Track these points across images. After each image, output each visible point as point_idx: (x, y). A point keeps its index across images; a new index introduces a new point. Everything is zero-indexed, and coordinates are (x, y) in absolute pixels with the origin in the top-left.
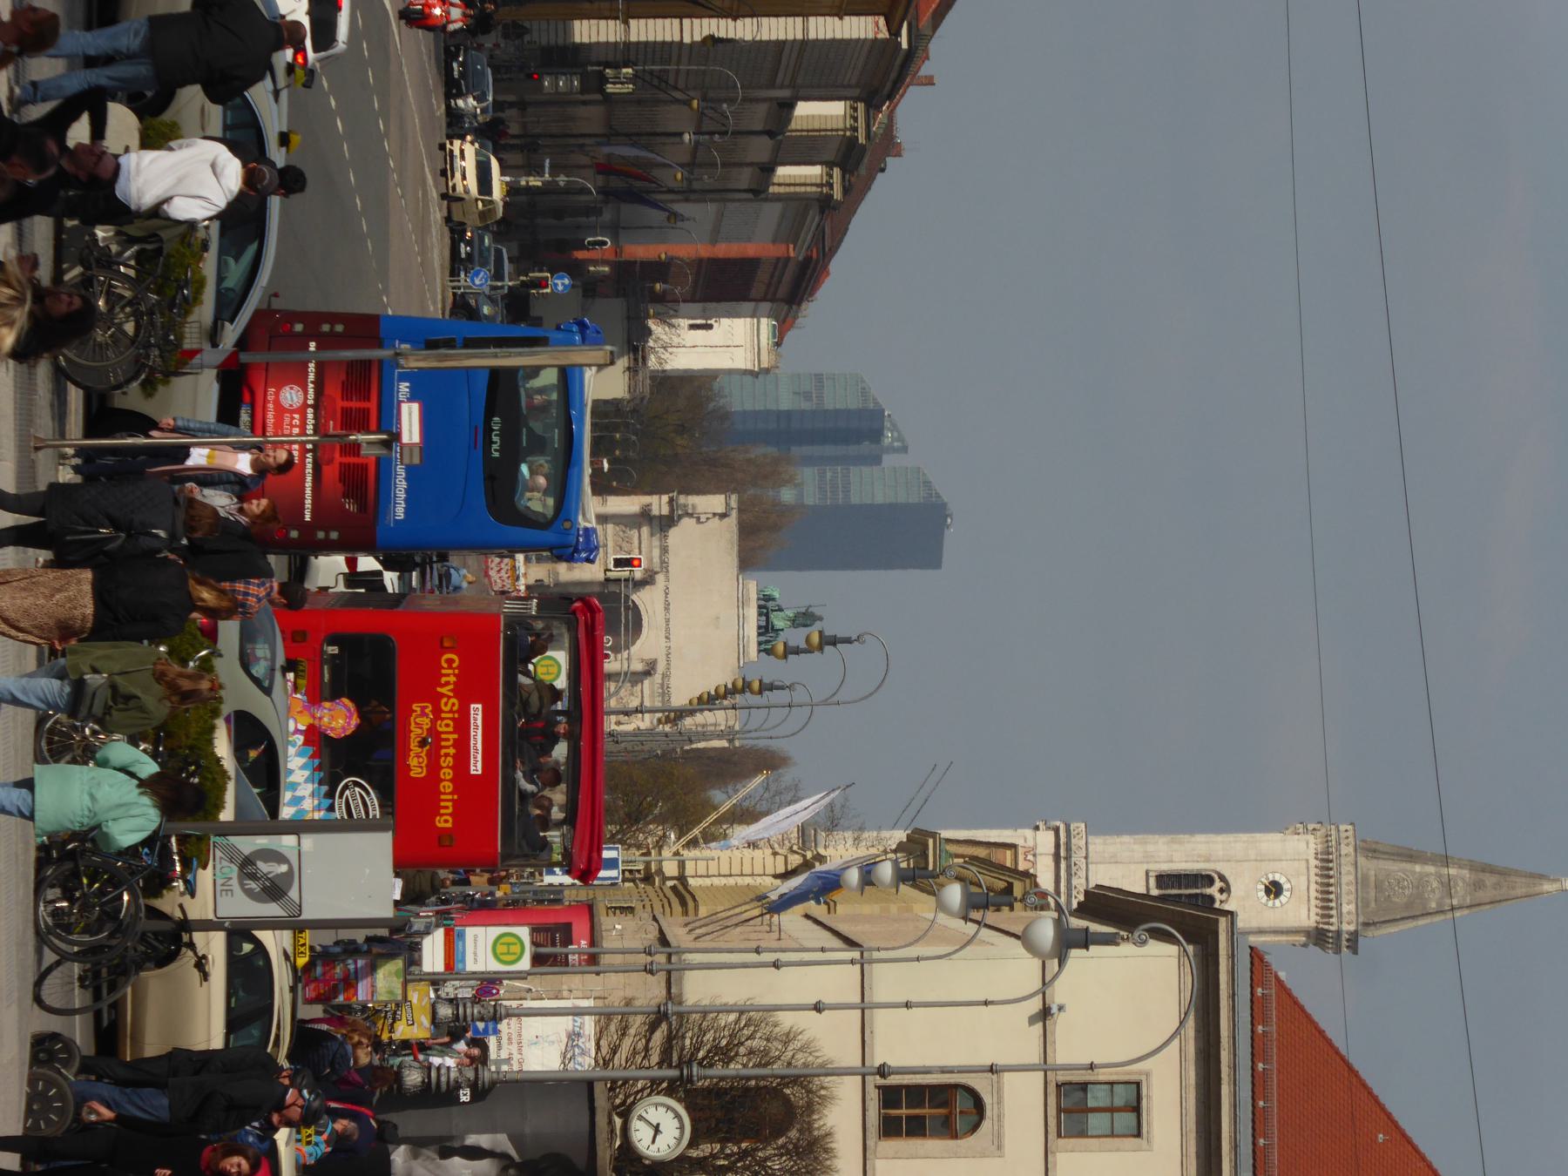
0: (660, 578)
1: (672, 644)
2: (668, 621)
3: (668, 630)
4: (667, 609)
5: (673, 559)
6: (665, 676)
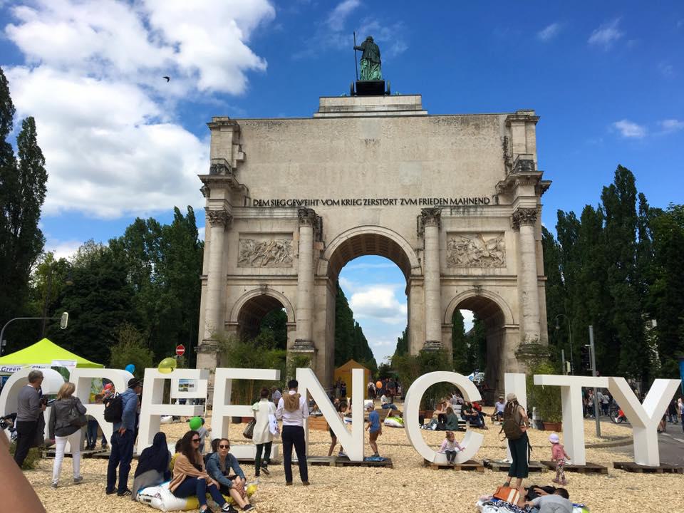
1: (399, 198)
2: (369, 202)
4: (354, 203)
5: (290, 196)
6: (442, 203)
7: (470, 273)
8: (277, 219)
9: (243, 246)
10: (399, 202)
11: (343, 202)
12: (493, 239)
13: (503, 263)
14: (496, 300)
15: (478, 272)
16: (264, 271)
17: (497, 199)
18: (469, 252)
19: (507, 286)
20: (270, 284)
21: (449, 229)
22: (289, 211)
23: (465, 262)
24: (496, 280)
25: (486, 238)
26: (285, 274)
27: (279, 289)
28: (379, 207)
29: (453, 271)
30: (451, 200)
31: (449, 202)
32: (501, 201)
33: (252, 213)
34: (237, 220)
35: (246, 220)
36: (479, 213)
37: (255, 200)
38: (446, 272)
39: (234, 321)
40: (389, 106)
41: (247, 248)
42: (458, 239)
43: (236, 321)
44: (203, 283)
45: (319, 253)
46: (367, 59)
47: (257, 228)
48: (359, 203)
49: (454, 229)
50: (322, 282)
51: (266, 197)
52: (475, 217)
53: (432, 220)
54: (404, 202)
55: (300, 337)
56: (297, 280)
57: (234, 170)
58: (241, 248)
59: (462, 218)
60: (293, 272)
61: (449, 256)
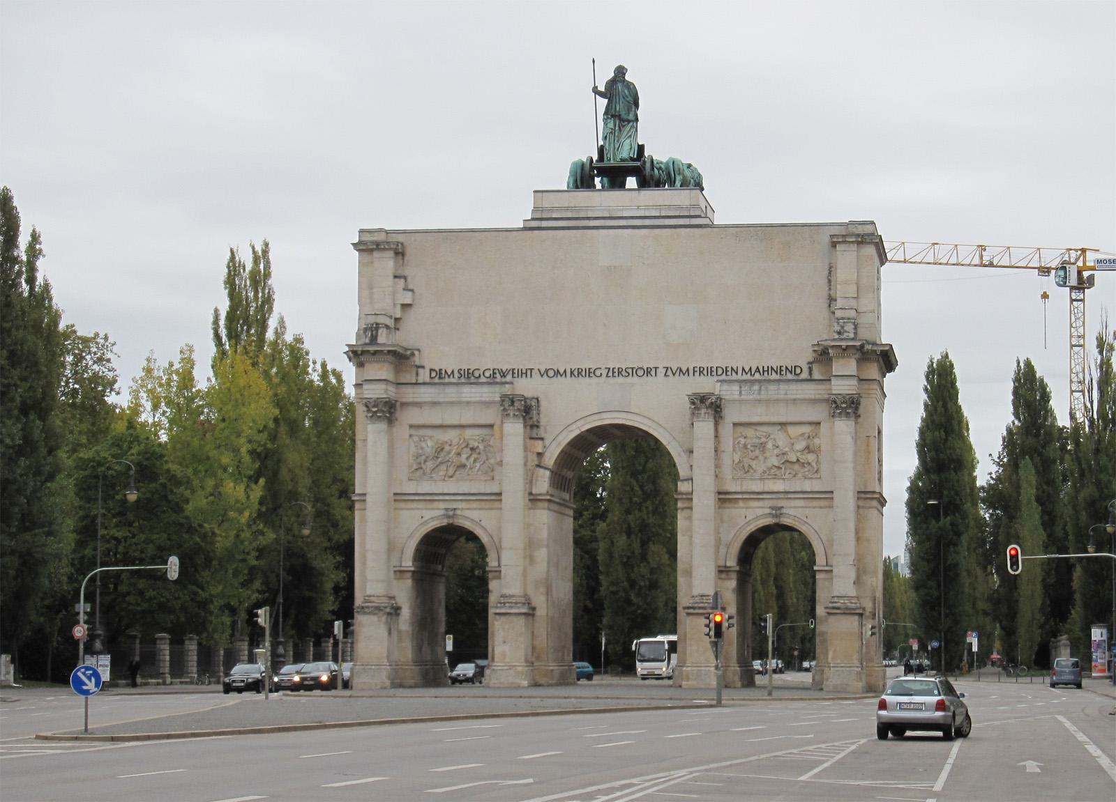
0: (525, 387)
1: (661, 365)
3: (633, 372)
4: (590, 373)
5: (486, 363)
7: (766, 489)
8: (468, 403)
9: (416, 446)
10: (661, 371)
11: (572, 373)
12: (803, 435)
13: (817, 470)
14: (803, 528)
15: (779, 486)
16: (450, 487)
17: (810, 370)
18: (768, 454)
19: (821, 507)
20: (460, 507)
21: (736, 420)
22: (486, 389)
23: (760, 470)
24: (804, 498)
25: (794, 431)
26: (482, 491)
27: (475, 515)
28: (629, 380)
29: (742, 485)
30: (743, 369)
31: (740, 372)
32: (816, 375)
33: (425, 394)
34: (403, 404)
35: (418, 405)
36: (783, 392)
37: (431, 370)
38: (731, 487)
39: (407, 565)
40: (647, 207)
41: (422, 448)
42: (750, 432)
43: (411, 564)
44: (357, 506)
45: (535, 457)
46: (613, 116)
47: (435, 417)
48: (598, 373)
49: (744, 418)
50: (540, 504)
51: (449, 365)
52: (777, 401)
53: (703, 411)
54: (669, 372)
55: (507, 591)
56: (501, 500)
57: (397, 320)
58: (413, 449)
59: (759, 401)
60: (496, 490)
61: (737, 460)
